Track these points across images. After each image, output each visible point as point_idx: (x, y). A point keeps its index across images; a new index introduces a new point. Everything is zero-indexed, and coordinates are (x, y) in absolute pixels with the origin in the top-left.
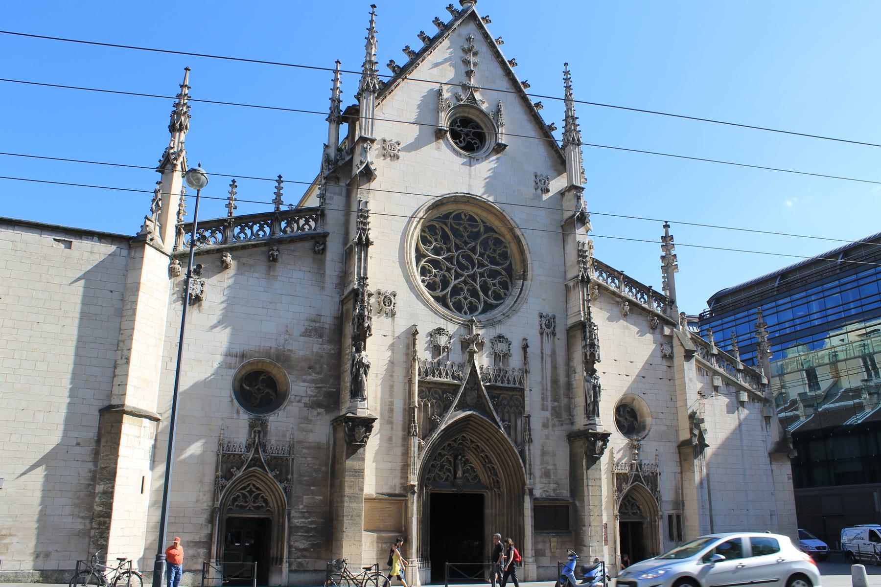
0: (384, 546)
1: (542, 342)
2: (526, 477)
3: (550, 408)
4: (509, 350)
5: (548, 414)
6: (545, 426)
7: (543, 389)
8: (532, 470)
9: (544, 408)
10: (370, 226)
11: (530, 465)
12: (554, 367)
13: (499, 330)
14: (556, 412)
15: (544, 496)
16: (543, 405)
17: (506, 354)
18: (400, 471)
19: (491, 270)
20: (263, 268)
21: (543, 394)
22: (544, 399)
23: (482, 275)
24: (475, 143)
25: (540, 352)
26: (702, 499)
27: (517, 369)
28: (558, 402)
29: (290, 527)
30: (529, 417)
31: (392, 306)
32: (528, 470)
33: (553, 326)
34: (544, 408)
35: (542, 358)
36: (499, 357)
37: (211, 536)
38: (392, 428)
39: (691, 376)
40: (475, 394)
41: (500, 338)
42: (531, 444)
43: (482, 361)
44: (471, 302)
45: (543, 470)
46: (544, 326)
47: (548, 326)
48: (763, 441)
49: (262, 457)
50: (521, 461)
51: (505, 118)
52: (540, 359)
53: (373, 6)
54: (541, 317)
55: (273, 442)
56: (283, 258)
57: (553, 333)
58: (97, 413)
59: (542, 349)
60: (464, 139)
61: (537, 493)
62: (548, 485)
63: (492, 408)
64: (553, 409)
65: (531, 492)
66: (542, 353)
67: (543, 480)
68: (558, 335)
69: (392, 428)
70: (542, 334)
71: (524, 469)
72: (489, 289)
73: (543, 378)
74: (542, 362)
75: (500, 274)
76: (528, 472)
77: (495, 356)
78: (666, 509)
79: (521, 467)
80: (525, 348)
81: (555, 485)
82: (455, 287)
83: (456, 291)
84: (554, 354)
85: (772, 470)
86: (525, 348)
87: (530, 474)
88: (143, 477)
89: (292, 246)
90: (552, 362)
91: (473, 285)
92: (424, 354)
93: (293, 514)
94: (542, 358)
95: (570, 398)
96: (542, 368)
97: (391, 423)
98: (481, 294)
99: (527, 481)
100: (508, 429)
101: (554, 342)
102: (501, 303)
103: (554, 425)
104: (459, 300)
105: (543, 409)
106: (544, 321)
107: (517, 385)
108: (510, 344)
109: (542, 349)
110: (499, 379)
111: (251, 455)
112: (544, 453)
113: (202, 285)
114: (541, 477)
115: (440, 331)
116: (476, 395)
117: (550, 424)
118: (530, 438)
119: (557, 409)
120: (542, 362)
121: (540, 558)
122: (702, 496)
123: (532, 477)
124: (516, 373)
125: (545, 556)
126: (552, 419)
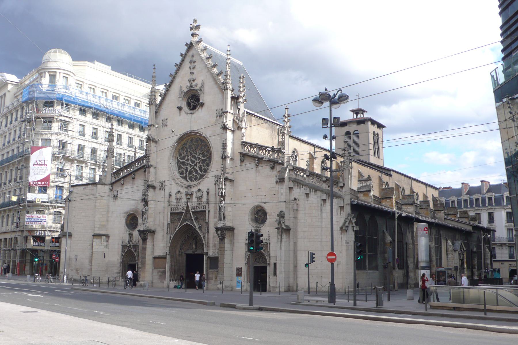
4: (202, 195)
7: (215, 209)
9: (215, 217)
10: (150, 160)
13: (200, 187)
15: (213, 255)
16: (215, 216)
17: (201, 197)
19: (203, 160)
20: (131, 182)
21: (215, 211)
22: (215, 213)
23: (199, 163)
24: (191, 107)
26: (280, 255)
29: (138, 268)
31: (164, 187)
34: (215, 217)
36: (200, 198)
37: (120, 270)
39: (282, 191)
41: (199, 190)
43: (194, 200)
48: (337, 221)
49: (131, 245)
51: (206, 88)
52: (214, 196)
53: (154, 65)
55: (134, 240)
56: (137, 177)
58: (92, 236)
60: (195, 103)
61: (211, 254)
65: (207, 253)
66: (215, 193)
67: (213, 248)
70: (215, 184)
74: (215, 197)
75: (207, 160)
78: (272, 261)
80: (208, 193)
82: (190, 171)
85: (341, 238)
86: (208, 193)
88: (105, 254)
89: (139, 172)
92: (174, 202)
93: (139, 263)
97: (163, 230)
111: (128, 245)
113: (117, 192)
114: (213, 247)
115: (179, 192)
121: (211, 280)
122: (280, 254)
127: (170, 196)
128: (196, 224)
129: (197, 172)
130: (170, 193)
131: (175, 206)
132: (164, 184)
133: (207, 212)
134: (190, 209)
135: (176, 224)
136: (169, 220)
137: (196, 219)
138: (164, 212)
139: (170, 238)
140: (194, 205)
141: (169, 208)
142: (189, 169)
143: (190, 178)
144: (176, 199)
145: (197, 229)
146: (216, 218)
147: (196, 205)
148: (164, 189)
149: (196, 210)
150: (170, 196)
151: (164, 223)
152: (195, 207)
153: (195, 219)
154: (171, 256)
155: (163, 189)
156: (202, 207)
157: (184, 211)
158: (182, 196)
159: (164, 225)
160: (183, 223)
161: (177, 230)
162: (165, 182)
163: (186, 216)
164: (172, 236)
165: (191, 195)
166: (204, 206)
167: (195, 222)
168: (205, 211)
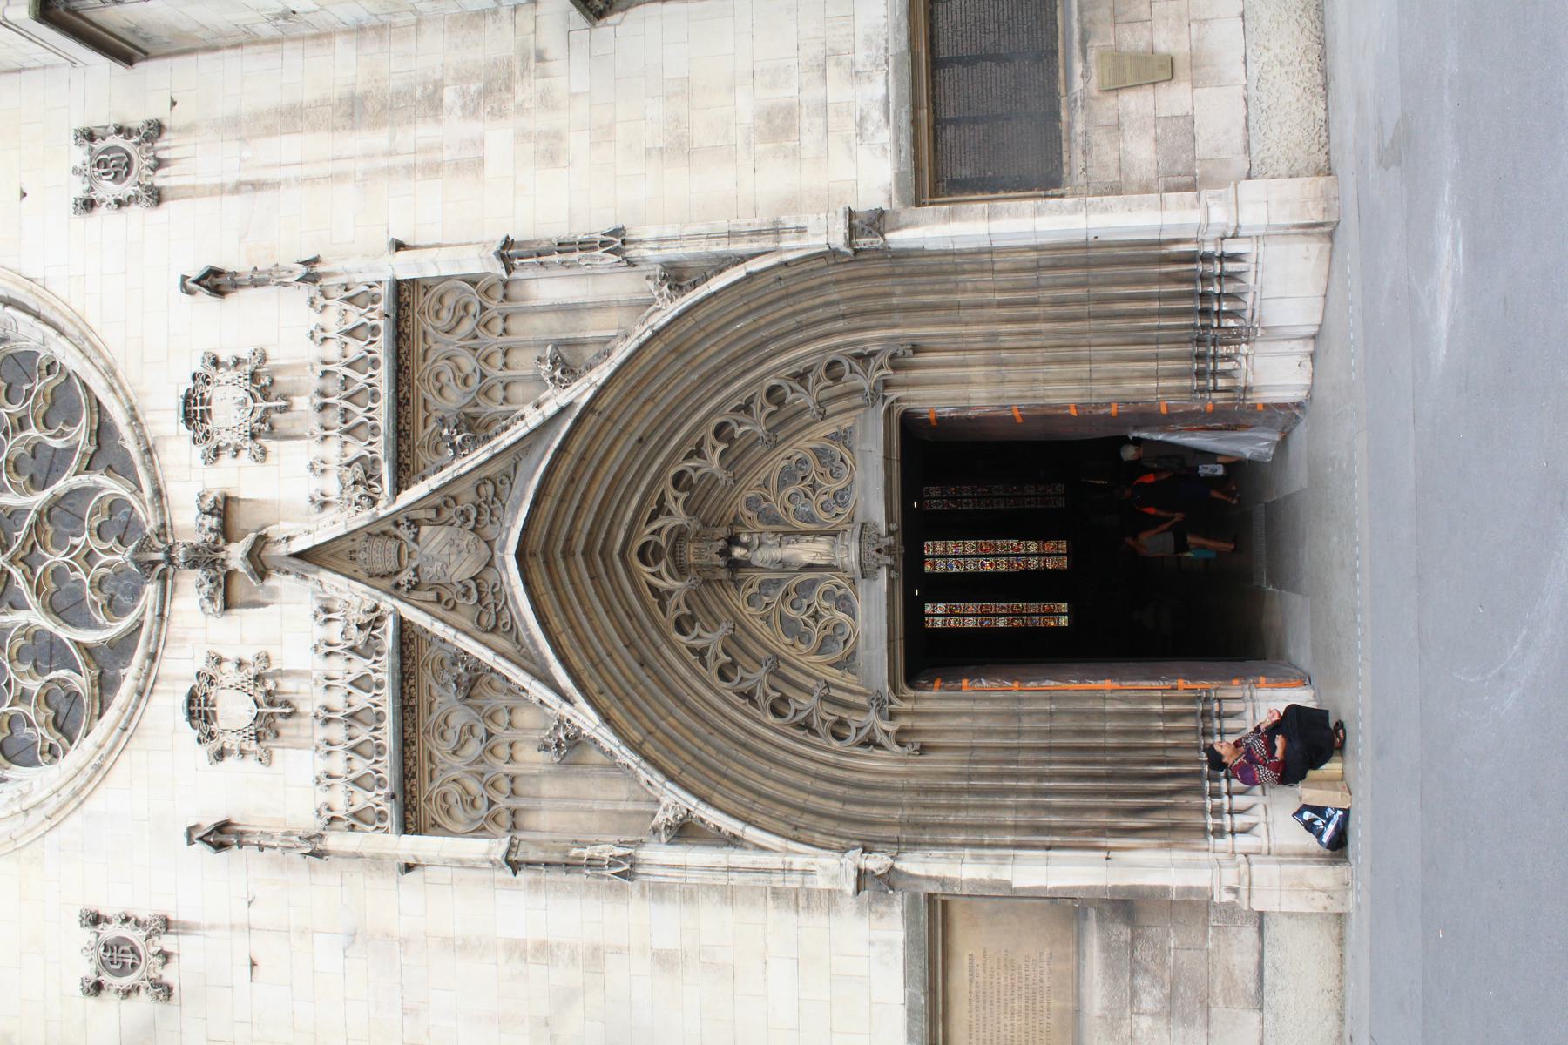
0: (1148, 1001)
1: (191, 192)
2: (793, 248)
3: (474, 128)
4: (238, 362)
5: (498, 138)
6: (550, 150)
7: (389, 171)
8: (757, 223)
11: (732, 235)
12: (291, 117)
13: (165, 421)
14: (486, 93)
16: (458, 166)
17: (254, 376)
18: (803, 916)
21: (410, 170)
25: (236, 197)
27: (313, 319)
28: (439, 86)
30: (508, 252)
31: (137, 936)
32: (755, 247)
33: (118, 141)
35: (256, 186)
38: (619, 951)
40: (434, 539)
42: (633, 233)
44: (99, 532)
45: (760, 147)
46: (126, 189)
47: (119, 167)
50: (717, 283)
52: (264, 197)
54: (89, 205)
57: (149, 138)
59: (221, 190)
62: (832, 119)
63: (481, 454)
64: (471, 110)
66: (238, 188)
68: (159, 111)
69: (619, 951)
70: (157, 197)
71: (755, 265)
72: (37, 449)
73: (337, 177)
74: (276, 185)
76: (767, 244)
77: (272, 433)
79: (750, 276)
81: (832, 71)
82: (52, 608)
83: (66, 607)
84: (238, 127)
87: (777, 231)
90: (270, 131)
91: (36, 526)
94: (256, 186)
95: (418, 23)
96: (302, 181)
98: (61, 486)
99: (816, 242)
100: (566, 367)
101: (189, 129)
102: (84, 385)
103: (546, 101)
104: (99, 585)
105: (478, 164)
106: (108, 189)
107: (379, 314)
108: (216, 363)
109: (221, 190)
110: (359, 415)
112: (680, 149)
115: (199, 710)
116: (443, 532)
117: (542, 121)
118: (603, 244)
119: (473, 88)
120: (276, 185)
121: (1203, 149)
123: (790, 221)
124: (332, 320)
125: (1190, 119)
126: (520, 109)
127: (221, 836)
128: (534, 419)
129: (64, 512)
130: (208, 823)
131: (338, 764)
132: (110, 932)
133: (406, 267)
134: (363, 518)
135: (525, 717)
136: (476, 848)
137: (474, 427)
138: (404, 942)
139: (684, 831)
140: (332, 486)
141: (366, 841)
142: (35, 616)
143: (115, 609)
144: (265, 759)
145: (580, 392)
146: (479, 143)
147: (332, 450)
148: (167, 924)
149: (381, 449)
150: (221, 836)
151: (516, 949)
152: (356, 449)
153: (477, 442)
154: (919, 835)
155: (167, 942)
156: (356, 349)
157: (388, 604)
158: (240, 664)
159: (544, 951)
160: (512, 632)
161: (586, 719)
162: (96, 920)
163: (442, 600)
164: (674, 801)
165: (223, 510)
166: (355, 317)
167: (506, 439)
168: (402, 290)
